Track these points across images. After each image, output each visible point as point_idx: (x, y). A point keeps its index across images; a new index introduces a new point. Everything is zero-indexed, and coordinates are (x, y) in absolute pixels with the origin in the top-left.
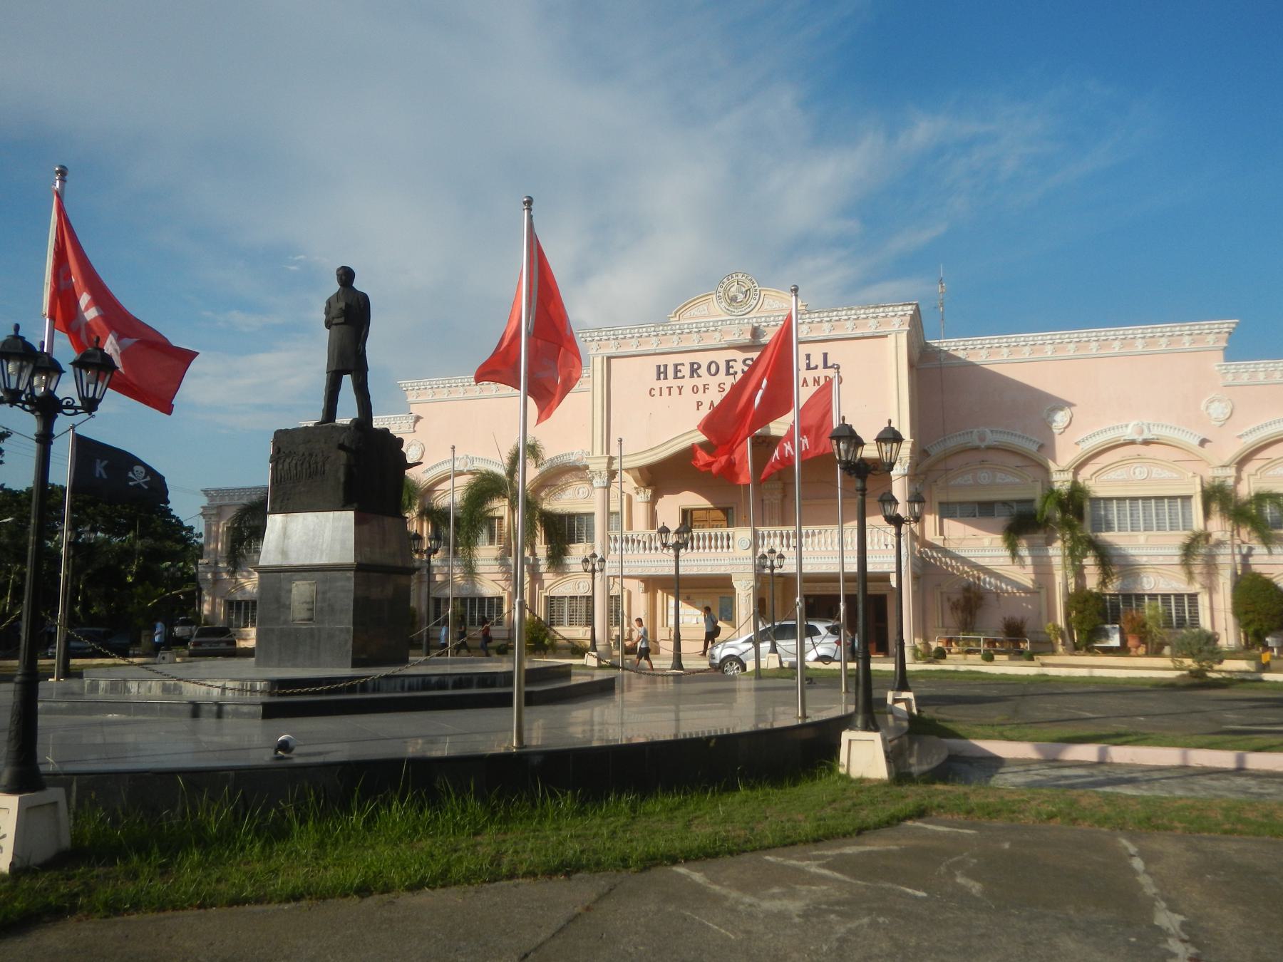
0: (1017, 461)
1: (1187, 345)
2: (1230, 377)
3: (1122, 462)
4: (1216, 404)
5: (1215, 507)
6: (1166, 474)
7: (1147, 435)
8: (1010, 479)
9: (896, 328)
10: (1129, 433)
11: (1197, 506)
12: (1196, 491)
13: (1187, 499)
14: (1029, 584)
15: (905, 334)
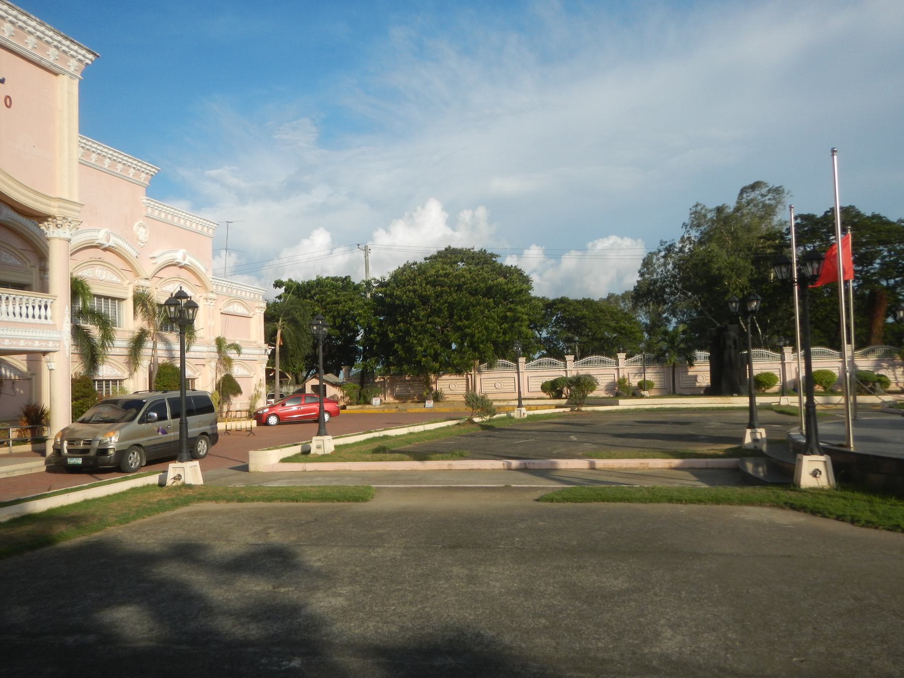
0: (17, 243)
1: (131, 176)
2: (150, 210)
3: (92, 263)
4: (142, 229)
5: (139, 309)
6: (115, 279)
7: (111, 243)
8: (13, 260)
9: (72, 70)
10: (101, 237)
11: (129, 305)
12: (130, 295)
13: (121, 300)
14: (24, 368)
15: (76, 82)
